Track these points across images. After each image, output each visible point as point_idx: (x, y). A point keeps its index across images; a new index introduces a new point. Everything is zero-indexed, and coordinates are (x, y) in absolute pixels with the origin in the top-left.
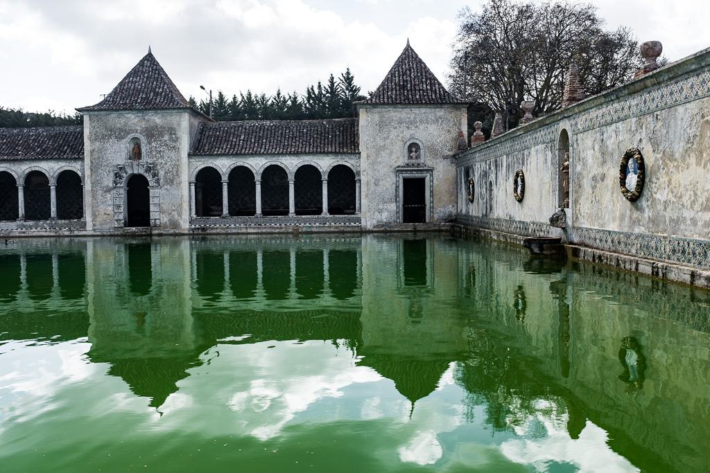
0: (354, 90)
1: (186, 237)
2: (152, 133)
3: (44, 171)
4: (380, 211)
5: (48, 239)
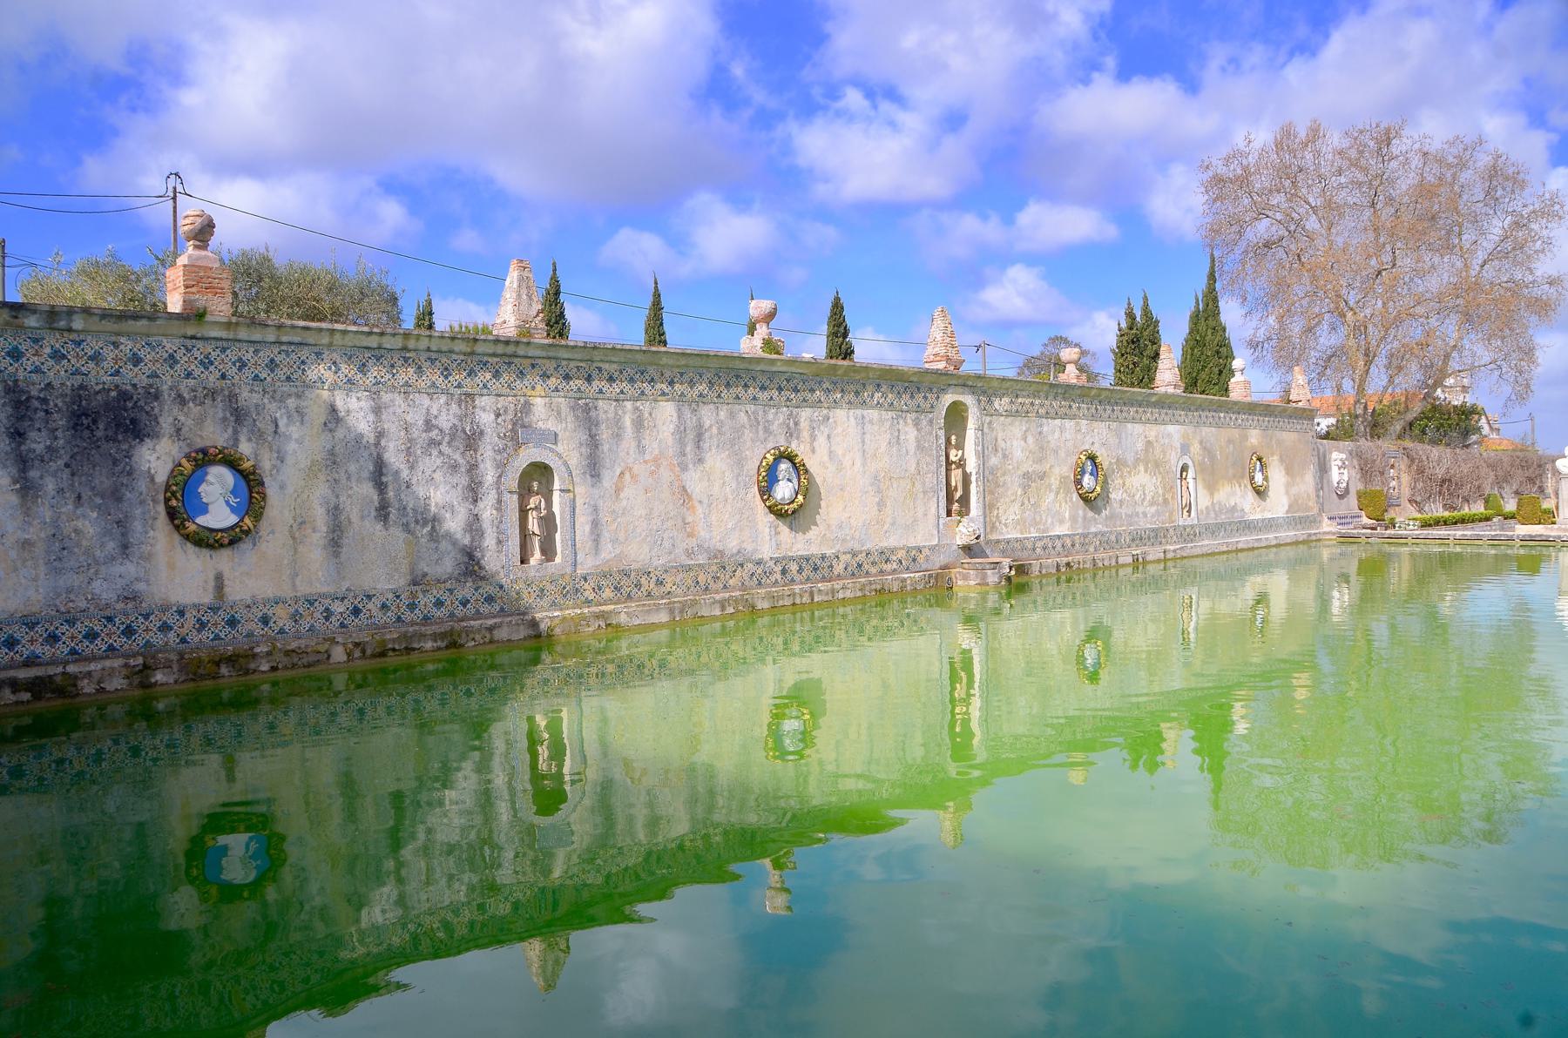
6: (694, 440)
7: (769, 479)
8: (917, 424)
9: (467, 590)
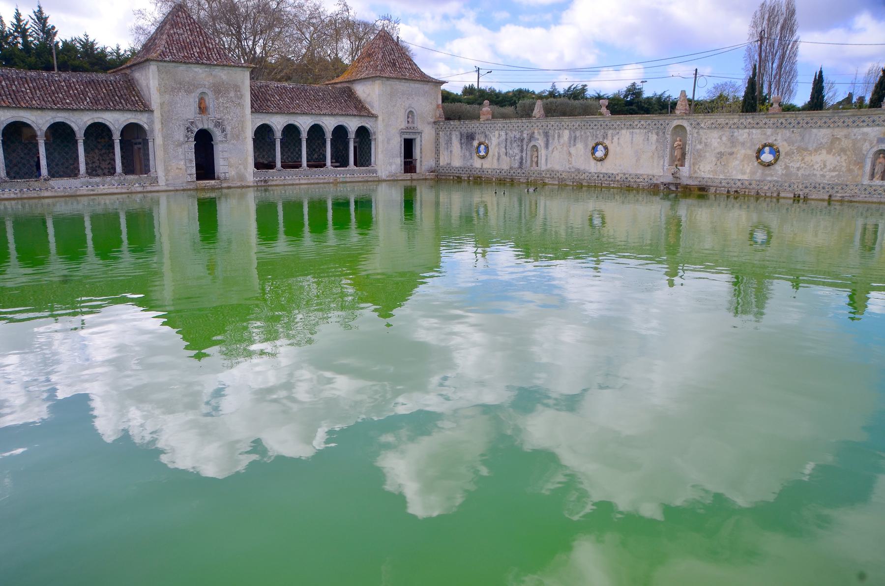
0: (49, 33)
1: (251, 189)
2: (219, 89)
3: (108, 123)
4: (391, 164)
5: (119, 196)
6: (574, 140)
7: (594, 149)
8: (657, 134)
9: (519, 171)
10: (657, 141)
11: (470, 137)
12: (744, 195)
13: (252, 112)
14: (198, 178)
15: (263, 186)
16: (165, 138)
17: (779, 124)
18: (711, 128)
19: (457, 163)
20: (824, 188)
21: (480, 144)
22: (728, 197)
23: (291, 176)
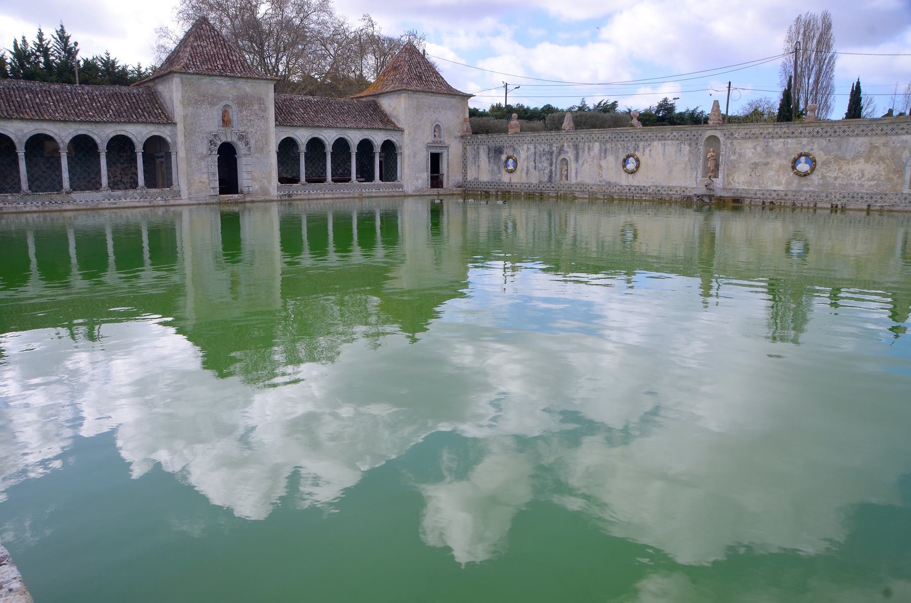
0: (71, 52)
1: (275, 203)
2: (243, 102)
3: (130, 136)
4: (417, 179)
6: (604, 152)
7: (625, 161)
8: (690, 145)
9: (548, 185)
10: (690, 152)
11: (499, 151)
12: (780, 206)
13: (276, 125)
14: (221, 192)
15: (287, 200)
16: (187, 150)
17: (815, 133)
18: (746, 138)
19: (485, 177)
20: (862, 198)
21: (508, 158)
22: (763, 208)
23: (315, 190)
